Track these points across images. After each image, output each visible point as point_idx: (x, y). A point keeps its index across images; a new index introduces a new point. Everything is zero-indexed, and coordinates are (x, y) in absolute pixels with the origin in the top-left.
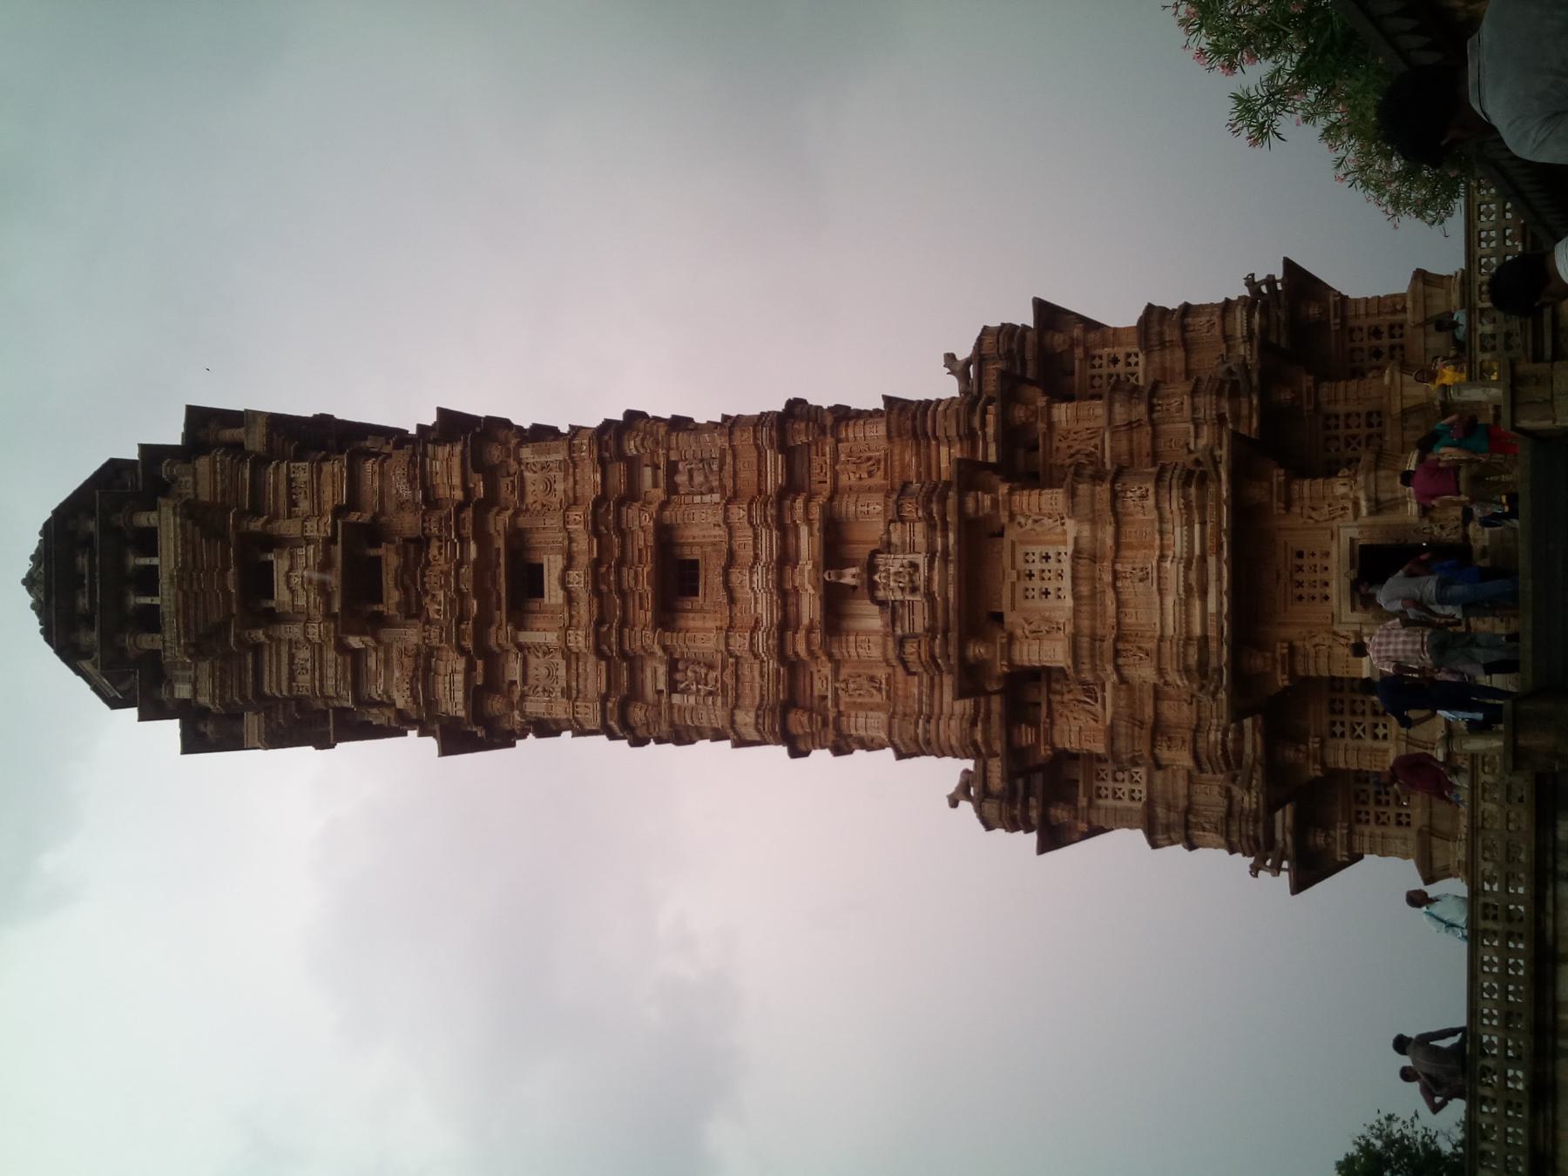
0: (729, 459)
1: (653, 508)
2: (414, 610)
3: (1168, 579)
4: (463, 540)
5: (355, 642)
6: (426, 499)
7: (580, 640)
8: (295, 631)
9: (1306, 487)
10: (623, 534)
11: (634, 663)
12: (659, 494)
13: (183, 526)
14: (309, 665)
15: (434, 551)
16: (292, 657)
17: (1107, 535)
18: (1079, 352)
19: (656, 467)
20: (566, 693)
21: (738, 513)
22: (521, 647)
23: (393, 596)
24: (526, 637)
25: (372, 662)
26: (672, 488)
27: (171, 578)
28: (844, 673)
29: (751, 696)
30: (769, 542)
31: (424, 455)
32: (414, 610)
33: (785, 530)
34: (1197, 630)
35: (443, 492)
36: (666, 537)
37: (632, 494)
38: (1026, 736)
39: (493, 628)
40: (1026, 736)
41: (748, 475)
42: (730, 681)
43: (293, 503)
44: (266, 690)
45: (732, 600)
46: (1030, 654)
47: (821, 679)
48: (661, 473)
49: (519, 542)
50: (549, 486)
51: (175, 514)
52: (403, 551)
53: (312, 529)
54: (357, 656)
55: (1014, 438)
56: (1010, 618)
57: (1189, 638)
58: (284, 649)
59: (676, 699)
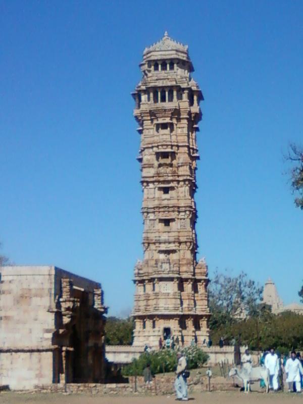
0: (185, 230)
1: (177, 217)
2: (160, 165)
3: (166, 306)
4: (172, 176)
5: (155, 149)
6: (179, 166)
7: (156, 203)
8: (156, 133)
9: (177, 321)
10: (173, 211)
11: (154, 212)
12: (180, 217)
13: (172, 109)
14: (149, 134)
15: (171, 169)
16: (151, 129)
17: (171, 297)
18: (201, 284)
19: (184, 215)
20: (148, 198)
21: (176, 234)
22: (155, 188)
23: (162, 161)
24: (157, 189)
25: (151, 150)
26: (181, 219)
27: (163, 107)
28: (154, 251)
29: (149, 235)
30: (172, 239)
31: (187, 165)
32: (160, 165)
33: (174, 242)
34: (160, 308)
35: (181, 169)
36: (173, 220)
37: (179, 212)
38: (147, 281)
39: (157, 183)
40: (147, 281)
41: (181, 234)
42: (151, 231)
43: (179, 128)
44: (145, 122)
45: (164, 232)
46: (156, 285)
47: (152, 247)
48: (183, 217)
49: (172, 188)
50: (182, 193)
51: (176, 107)
52: (170, 164)
53: (174, 138)
54: (152, 147)
55: (186, 280)
56: (161, 283)
57: (159, 307)
58: (152, 127)
59: (148, 221)
